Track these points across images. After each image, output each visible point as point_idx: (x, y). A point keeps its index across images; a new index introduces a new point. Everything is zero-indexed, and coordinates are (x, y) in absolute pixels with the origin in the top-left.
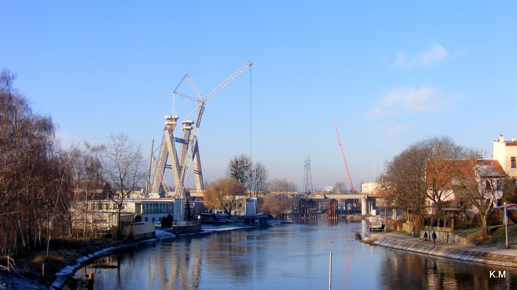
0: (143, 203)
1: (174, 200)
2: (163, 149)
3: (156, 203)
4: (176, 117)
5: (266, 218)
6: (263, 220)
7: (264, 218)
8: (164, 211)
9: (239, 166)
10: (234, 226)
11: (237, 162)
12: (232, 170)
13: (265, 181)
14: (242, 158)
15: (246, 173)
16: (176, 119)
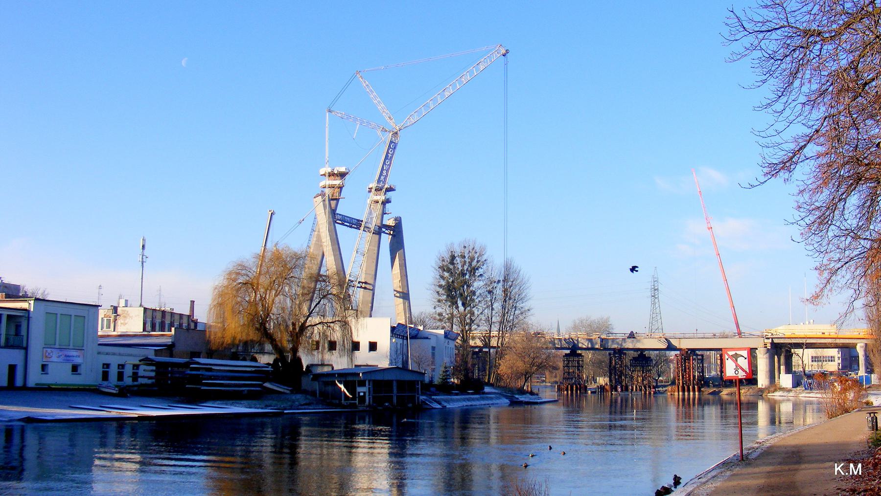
1: (32, 302)
2: (315, 239)
4: (343, 169)
6: (395, 388)
11: (453, 257)
13: (521, 305)
14: (465, 247)
15: (478, 285)
16: (342, 175)
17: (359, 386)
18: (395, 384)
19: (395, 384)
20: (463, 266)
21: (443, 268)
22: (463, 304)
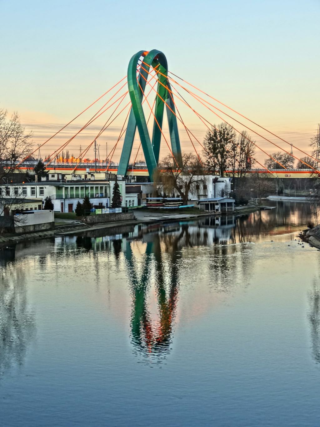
3: (84, 186)
5: (231, 203)
6: (226, 205)
7: (228, 203)
8: (97, 195)
9: (219, 139)
10: (191, 214)
12: (209, 143)
15: (228, 147)
17: (216, 205)
18: (226, 204)
19: (226, 204)
20: (219, 137)
21: (211, 139)
22: (222, 157)
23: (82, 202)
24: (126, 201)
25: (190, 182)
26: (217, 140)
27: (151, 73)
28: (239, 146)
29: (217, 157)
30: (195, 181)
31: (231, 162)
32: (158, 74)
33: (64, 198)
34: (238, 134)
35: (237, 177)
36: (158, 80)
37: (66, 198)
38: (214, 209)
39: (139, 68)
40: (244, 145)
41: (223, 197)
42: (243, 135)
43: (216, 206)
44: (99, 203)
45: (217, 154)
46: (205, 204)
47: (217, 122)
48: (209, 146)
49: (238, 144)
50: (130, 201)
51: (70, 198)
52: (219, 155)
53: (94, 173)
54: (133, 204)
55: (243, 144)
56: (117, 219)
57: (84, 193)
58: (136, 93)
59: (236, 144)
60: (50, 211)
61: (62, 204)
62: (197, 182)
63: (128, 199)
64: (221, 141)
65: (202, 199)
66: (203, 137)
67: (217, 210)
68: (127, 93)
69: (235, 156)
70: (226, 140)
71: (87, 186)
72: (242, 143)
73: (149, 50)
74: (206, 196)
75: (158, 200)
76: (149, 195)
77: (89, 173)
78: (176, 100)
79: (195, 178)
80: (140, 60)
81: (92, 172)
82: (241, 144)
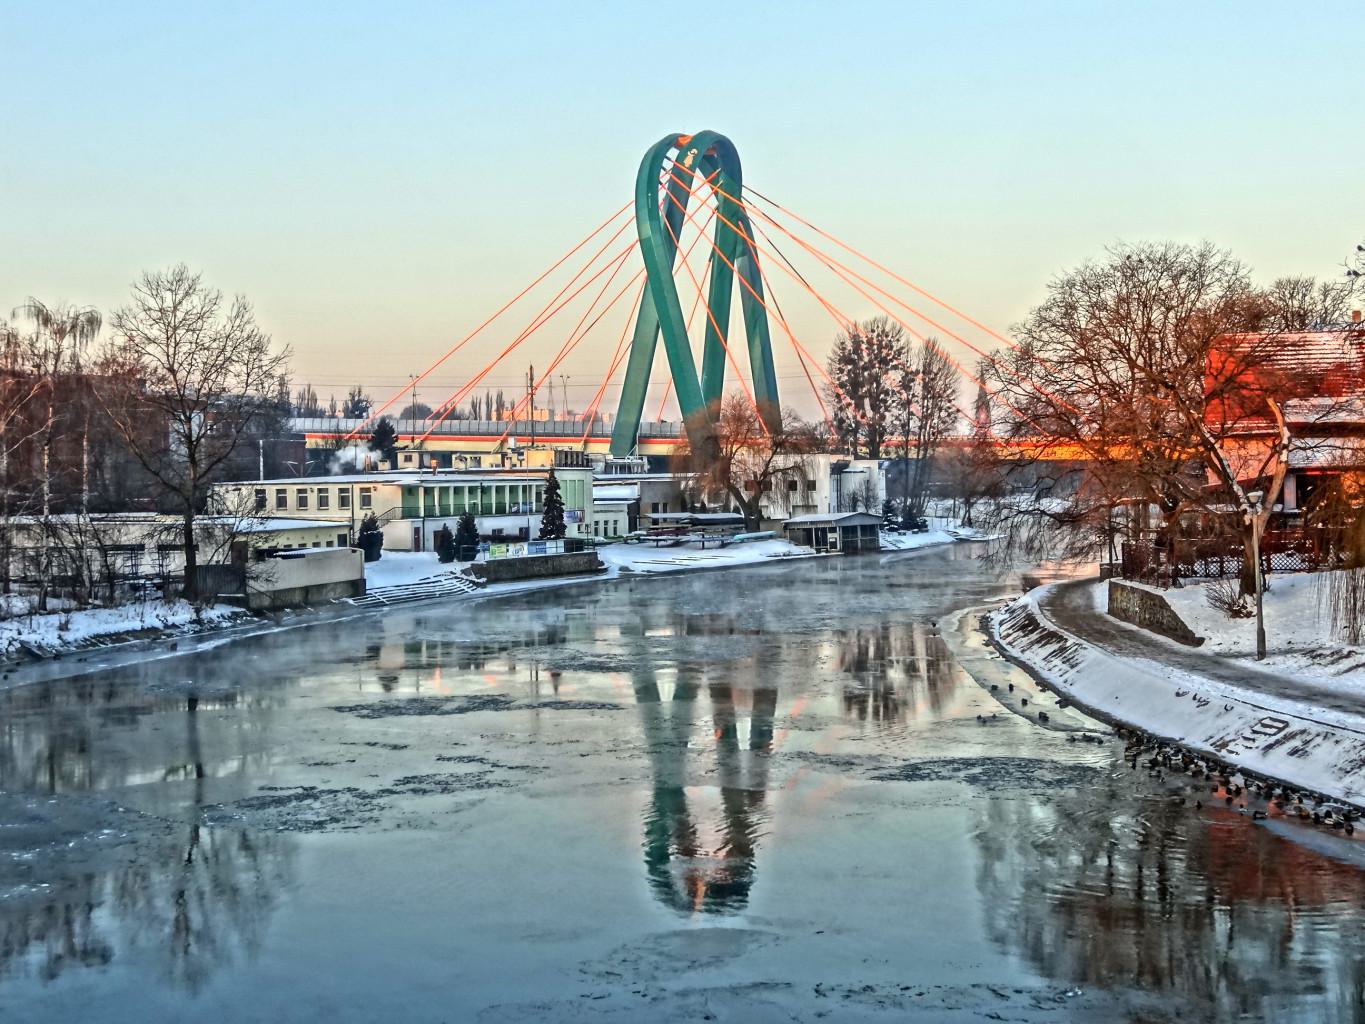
0: (425, 485)
3: (478, 484)
7: (863, 528)
8: (514, 509)
9: (866, 359)
12: (841, 371)
15: (892, 379)
22: (874, 408)
23: (453, 524)
24: (597, 523)
25: (765, 474)
26: (862, 363)
27: (698, 193)
28: (921, 375)
29: (859, 406)
30: (778, 471)
31: (897, 418)
32: (716, 193)
33: (422, 514)
34: (917, 345)
35: (915, 456)
36: (717, 208)
37: (429, 514)
38: (825, 543)
39: (665, 178)
40: (932, 376)
41: (854, 510)
42: (930, 348)
43: (829, 535)
44: (521, 529)
45: (862, 398)
46: (804, 530)
47: (864, 315)
48: (839, 379)
49: (917, 372)
50: (606, 522)
51: (441, 516)
52: (867, 402)
53: (528, 448)
54: (615, 529)
55: (930, 372)
56: (550, 571)
57: (479, 501)
58: (657, 242)
59: (912, 373)
60: (354, 551)
61: (417, 530)
62: (784, 471)
63: (601, 517)
64: (869, 366)
65: (801, 517)
66: (823, 354)
67: (833, 545)
68: (632, 246)
69: (909, 402)
70: (884, 361)
71: (485, 484)
72: (927, 371)
73: (691, 130)
74: (809, 508)
75: (677, 521)
76: (660, 507)
77: (513, 450)
78: (763, 262)
79: (780, 461)
80: (669, 159)
81: (524, 448)
82: (924, 372)
